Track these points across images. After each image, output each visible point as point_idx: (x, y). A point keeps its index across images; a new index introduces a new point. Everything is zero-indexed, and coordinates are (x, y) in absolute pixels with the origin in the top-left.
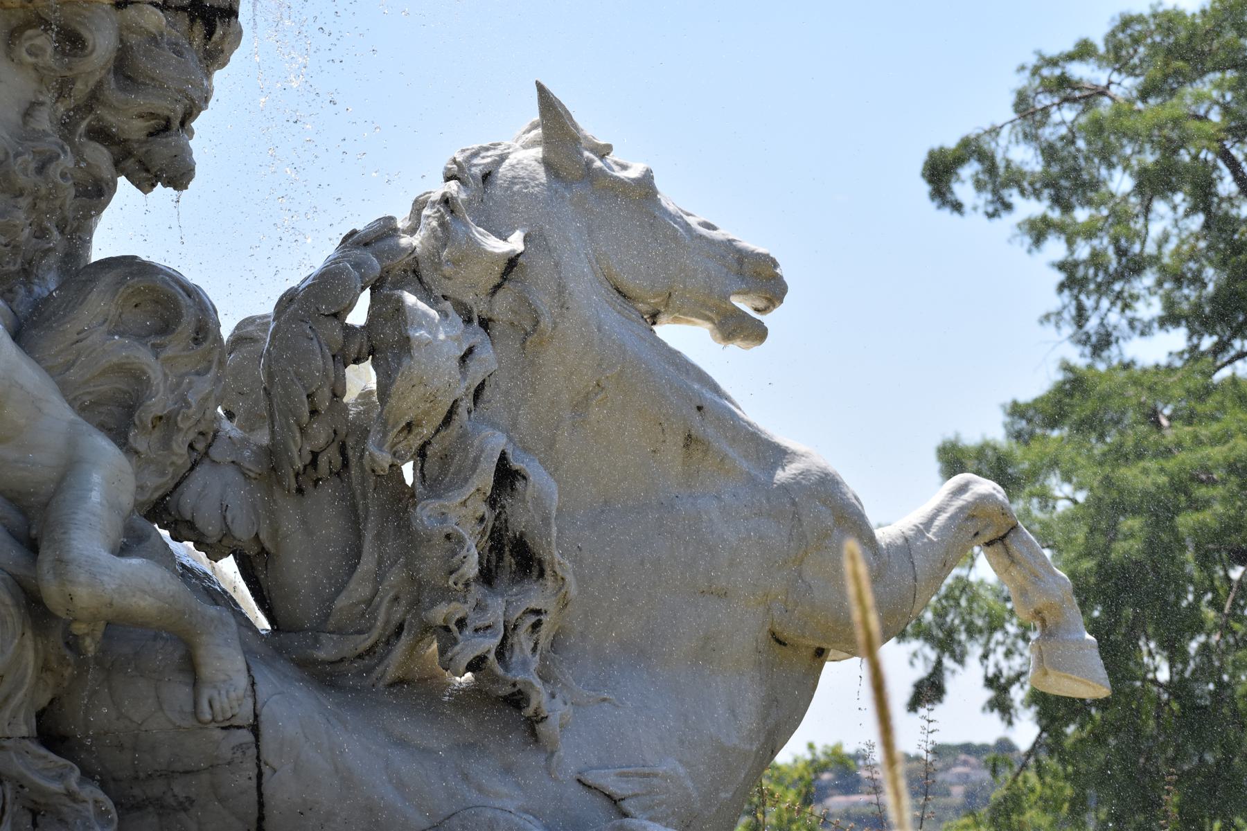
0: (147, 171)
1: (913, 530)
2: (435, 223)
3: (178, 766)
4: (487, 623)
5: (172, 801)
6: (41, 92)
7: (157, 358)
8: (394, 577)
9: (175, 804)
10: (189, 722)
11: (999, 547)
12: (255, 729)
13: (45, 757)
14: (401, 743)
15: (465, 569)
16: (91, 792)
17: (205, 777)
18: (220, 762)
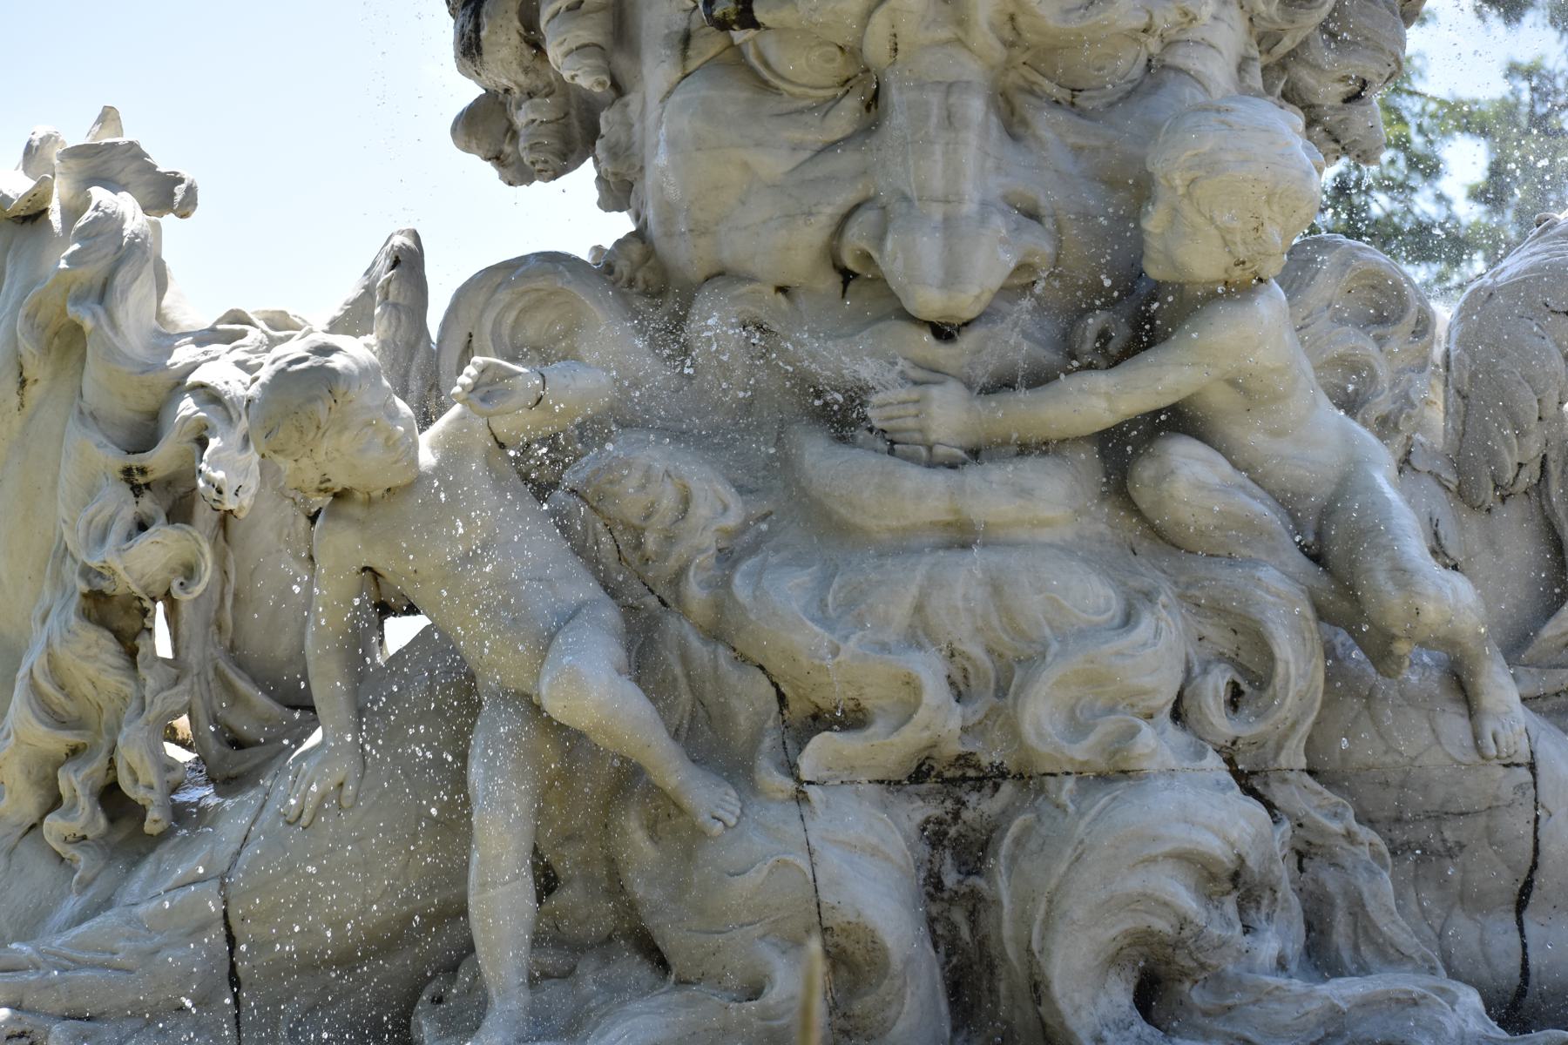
0: (1337, 141)
3: (1453, 808)
5: (1439, 846)
6: (1252, 46)
7: (1381, 351)
9: (1441, 849)
10: (1473, 757)
12: (1532, 767)
13: (1321, 793)
16: (1365, 834)
17: (1482, 821)
18: (1500, 803)
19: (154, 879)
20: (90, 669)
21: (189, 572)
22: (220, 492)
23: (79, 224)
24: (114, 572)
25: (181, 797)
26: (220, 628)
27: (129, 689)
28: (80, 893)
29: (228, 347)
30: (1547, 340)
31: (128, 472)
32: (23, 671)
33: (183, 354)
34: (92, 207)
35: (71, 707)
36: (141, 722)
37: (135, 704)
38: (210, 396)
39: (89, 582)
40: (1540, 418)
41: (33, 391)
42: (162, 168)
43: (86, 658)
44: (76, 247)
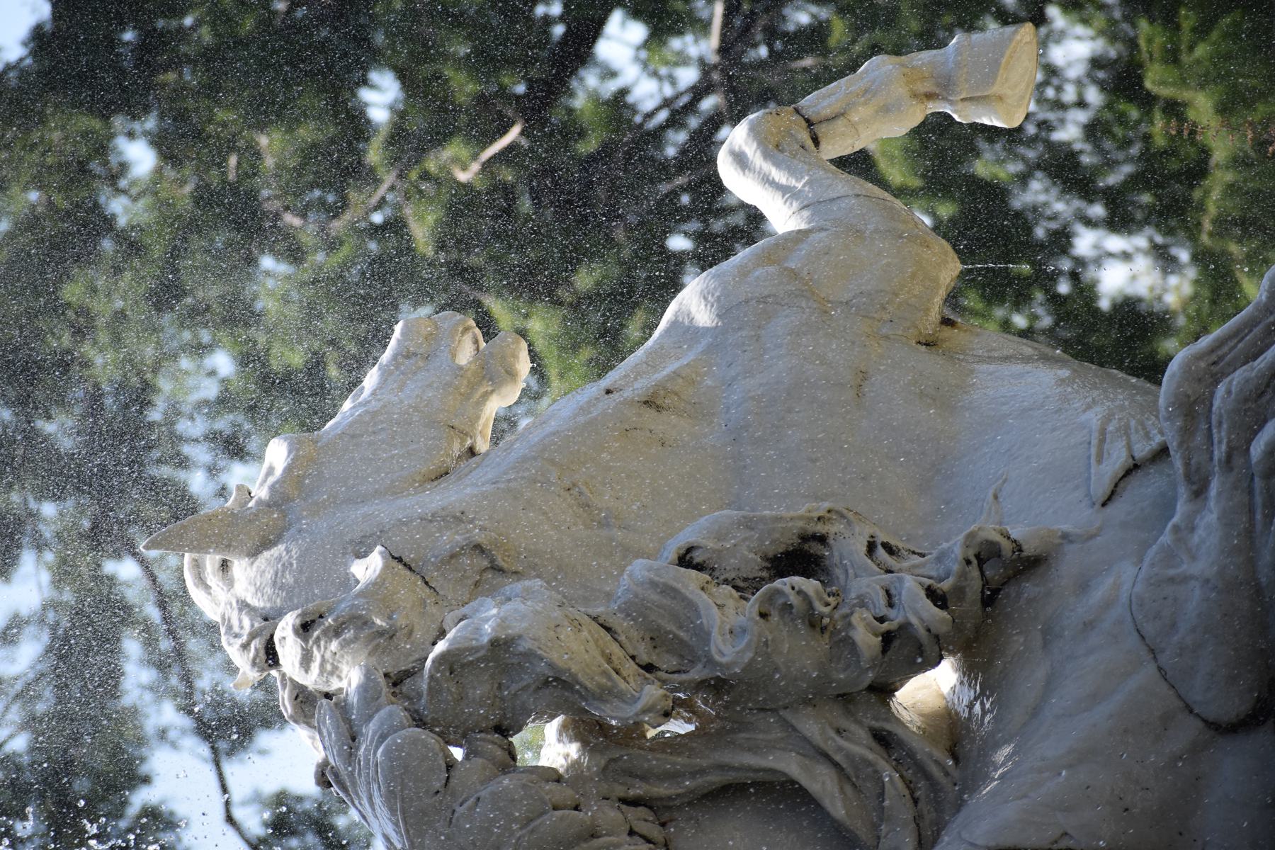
1: (791, 204)
2: (334, 646)
4: (882, 593)
8: (811, 726)
11: (821, 130)
14: (1035, 712)
15: (811, 593)
30: (483, 794)
40: (576, 808)
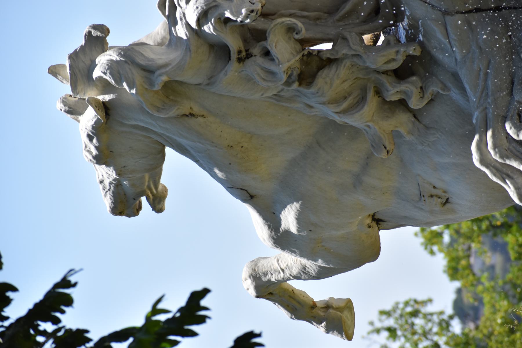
19: (443, 50)
20: (337, 82)
21: (291, 29)
22: (252, 11)
23: (113, 82)
24: (289, 68)
25: (403, 39)
26: (318, 19)
27: (348, 63)
28: (449, 90)
29: (178, 8)
31: (240, 60)
32: (338, 119)
33: (181, 31)
34: (105, 77)
35: (355, 94)
36: (364, 56)
37: (355, 59)
38: (203, 18)
39: (294, 82)
41: (196, 110)
42: (83, 42)
43: (331, 84)
44: (125, 85)
